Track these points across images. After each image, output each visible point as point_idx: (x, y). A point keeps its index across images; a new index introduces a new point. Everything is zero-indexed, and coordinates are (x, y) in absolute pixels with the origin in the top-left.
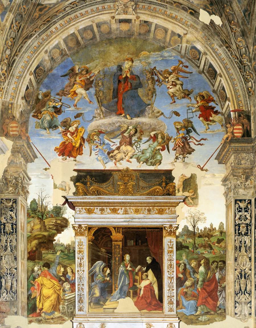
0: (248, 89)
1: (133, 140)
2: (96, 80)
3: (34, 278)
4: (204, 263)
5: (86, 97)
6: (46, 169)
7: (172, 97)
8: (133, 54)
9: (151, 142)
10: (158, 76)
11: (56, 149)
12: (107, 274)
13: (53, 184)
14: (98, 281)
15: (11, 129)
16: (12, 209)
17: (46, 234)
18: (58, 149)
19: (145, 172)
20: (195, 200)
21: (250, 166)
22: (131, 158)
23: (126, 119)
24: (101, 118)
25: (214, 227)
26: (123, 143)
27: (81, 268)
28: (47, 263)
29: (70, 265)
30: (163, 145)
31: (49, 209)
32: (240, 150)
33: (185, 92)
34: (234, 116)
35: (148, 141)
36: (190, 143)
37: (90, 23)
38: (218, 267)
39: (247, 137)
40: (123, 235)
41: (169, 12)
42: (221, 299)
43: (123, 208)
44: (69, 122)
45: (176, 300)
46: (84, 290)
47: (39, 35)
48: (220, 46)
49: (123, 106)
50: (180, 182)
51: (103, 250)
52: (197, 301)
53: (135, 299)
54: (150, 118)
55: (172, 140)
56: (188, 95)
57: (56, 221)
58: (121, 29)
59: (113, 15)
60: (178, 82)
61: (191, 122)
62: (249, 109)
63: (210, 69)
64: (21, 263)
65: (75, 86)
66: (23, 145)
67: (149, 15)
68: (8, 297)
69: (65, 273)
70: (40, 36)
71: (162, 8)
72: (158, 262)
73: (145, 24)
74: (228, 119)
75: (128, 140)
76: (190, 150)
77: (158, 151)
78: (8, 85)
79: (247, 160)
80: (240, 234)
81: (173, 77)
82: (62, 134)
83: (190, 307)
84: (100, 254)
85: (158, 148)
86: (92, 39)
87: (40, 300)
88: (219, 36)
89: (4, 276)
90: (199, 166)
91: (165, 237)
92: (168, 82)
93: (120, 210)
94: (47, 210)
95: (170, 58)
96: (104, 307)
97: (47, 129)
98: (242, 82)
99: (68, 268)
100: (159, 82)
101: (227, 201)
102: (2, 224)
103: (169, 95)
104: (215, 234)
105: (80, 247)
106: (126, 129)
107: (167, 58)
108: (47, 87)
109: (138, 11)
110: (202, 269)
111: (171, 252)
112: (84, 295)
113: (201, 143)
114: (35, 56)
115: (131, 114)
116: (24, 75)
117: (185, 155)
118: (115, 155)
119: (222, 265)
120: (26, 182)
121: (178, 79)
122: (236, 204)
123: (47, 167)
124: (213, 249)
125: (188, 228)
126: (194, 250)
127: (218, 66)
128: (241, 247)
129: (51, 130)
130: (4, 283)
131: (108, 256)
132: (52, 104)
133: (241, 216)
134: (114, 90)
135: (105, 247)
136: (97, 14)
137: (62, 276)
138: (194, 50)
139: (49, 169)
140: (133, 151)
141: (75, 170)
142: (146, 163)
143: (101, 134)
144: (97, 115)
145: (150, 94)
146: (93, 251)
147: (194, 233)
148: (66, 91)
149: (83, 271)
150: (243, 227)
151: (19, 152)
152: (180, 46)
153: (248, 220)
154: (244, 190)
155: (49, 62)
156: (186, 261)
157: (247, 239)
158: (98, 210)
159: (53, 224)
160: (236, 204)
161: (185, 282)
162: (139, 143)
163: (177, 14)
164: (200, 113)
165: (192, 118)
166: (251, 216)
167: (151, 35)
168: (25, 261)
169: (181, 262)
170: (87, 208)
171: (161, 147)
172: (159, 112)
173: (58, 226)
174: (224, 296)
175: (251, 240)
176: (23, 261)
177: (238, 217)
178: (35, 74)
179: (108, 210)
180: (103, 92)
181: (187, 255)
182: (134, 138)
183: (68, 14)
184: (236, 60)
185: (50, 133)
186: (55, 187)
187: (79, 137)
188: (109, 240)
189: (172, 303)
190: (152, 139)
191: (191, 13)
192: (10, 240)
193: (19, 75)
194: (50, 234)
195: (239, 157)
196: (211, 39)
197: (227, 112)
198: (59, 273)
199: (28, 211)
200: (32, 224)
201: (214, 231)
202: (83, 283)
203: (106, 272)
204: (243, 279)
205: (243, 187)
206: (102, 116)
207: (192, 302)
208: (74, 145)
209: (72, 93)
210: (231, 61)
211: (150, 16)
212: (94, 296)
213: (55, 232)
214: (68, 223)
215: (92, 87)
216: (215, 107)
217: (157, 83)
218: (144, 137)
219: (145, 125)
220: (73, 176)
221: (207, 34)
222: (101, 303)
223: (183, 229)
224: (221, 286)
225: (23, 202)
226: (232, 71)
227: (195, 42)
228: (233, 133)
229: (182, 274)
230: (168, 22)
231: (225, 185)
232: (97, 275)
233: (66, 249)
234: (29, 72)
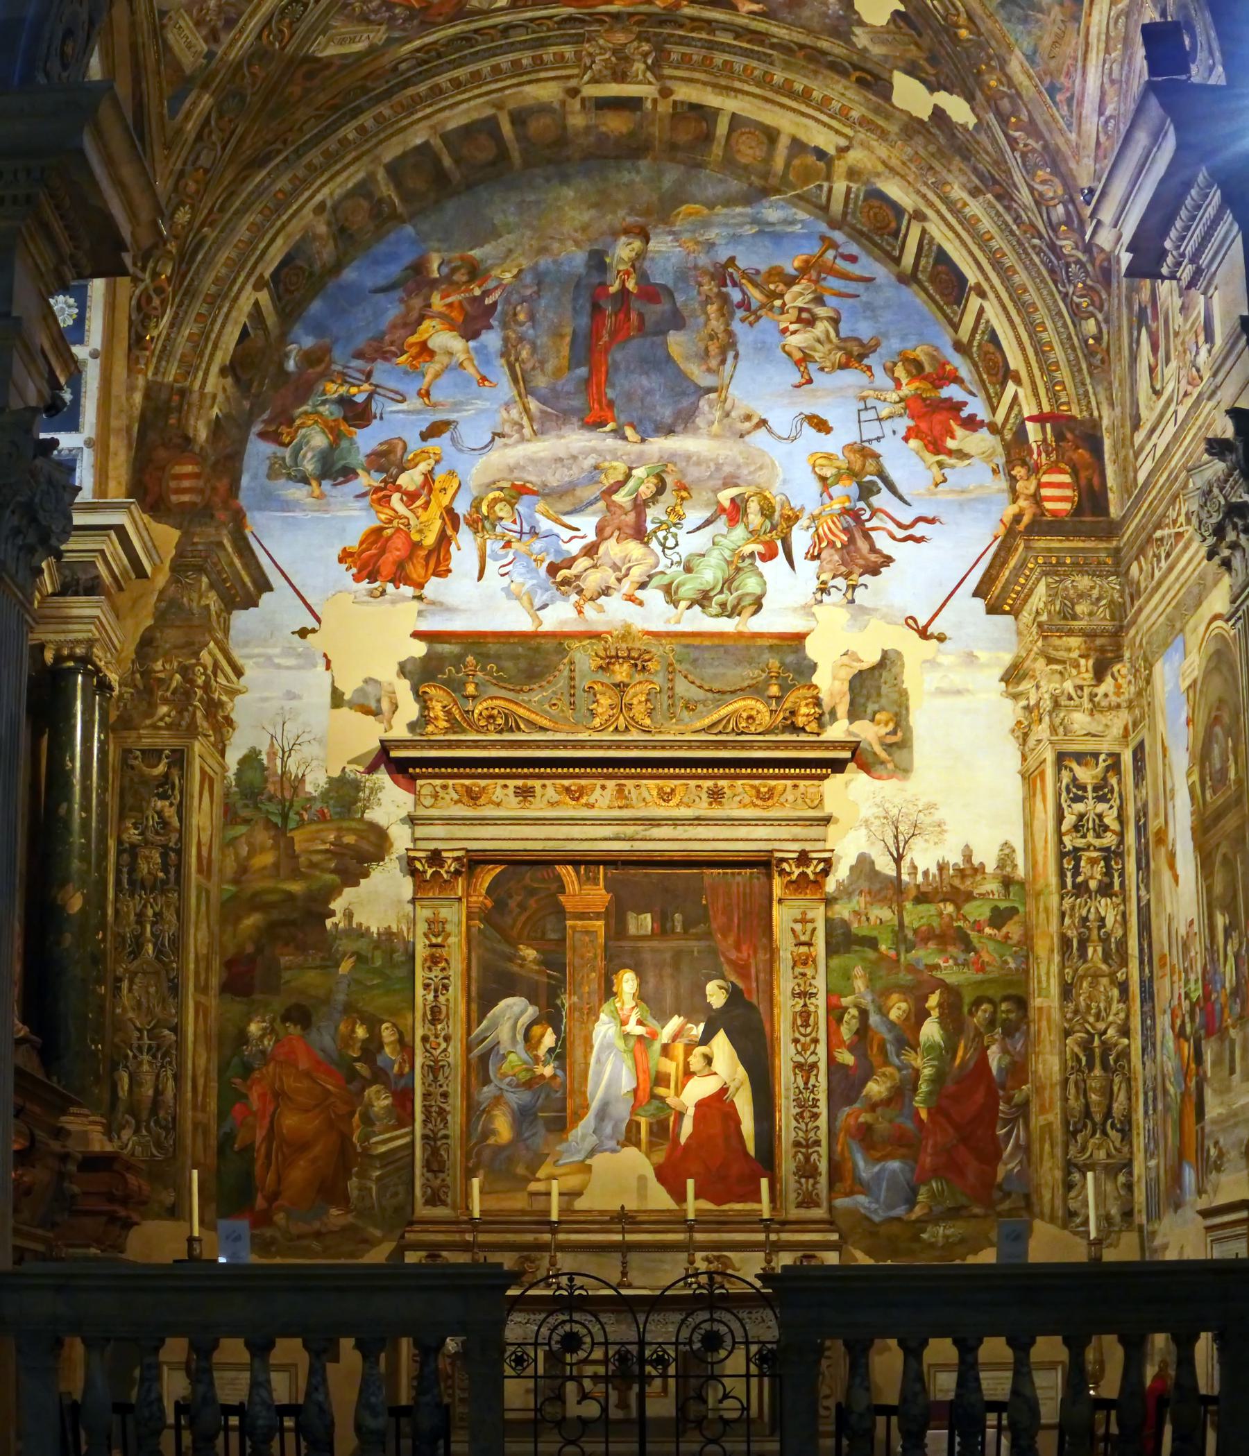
0: (1086, 341)
1: (649, 519)
2: (507, 301)
4: (940, 1005)
5: (466, 364)
6: (303, 633)
7: (797, 363)
8: (647, 212)
9: (721, 524)
10: (744, 293)
11: (345, 556)
12: (542, 1051)
13: (329, 690)
15: (173, 484)
16: (164, 787)
17: (296, 887)
18: (351, 555)
19: (697, 641)
20: (899, 755)
21: (1109, 625)
22: (643, 586)
23: (620, 442)
24: (523, 439)
25: (976, 861)
26: (608, 531)
30: (767, 538)
31: (309, 788)
32: (1068, 561)
33: (849, 345)
34: (1040, 437)
35: (708, 523)
36: (873, 534)
37: (489, 112)
38: (998, 1023)
39: (1093, 515)
41: (779, 77)
42: (1012, 1155)
43: (611, 784)
44: (399, 453)
45: (830, 1160)
46: (449, 1117)
47: (296, 151)
48: (975, 193)
49: (611, 394)
50: (837, 683)
51: (530, 954)
52: (916, 1161)
53: (660, 1157)
54: (716, 436)
55: (804, 521)
56: (861, 357)
57: (338, 838)
58: (604, 129)
59: (573, 83)
60: (820, 311)
61: (876, 456)
62: (1096, 414)
63: (940, 268)
64: (198, 1005)
65: (427, 324)
66: (221, 545)
67: (705, 83)
68: (139, 1143)
70: (299, 157)
71: (754, 64)
72: (755, 1001)
73: (692, 114)
74: (1016, 449)
75: (631, 518)
76: (873, 557)
77: (748, 561)
78: (172, 325)
79: (1098, 600)
80: (1081, 889)
81: (802, 294)
82: (368, 499)
83: (888, 1189)
85: (747, 549)
86: (493, 163)
87: (268, 1155)
88: (966, 158)
89: (127, 1056)
90: (910, 621)
91: (780, 901)
92: (783, 310)
93: (598, 790)
94: (302, 795)
95: (789, 229)
96: (534, 1186)
97: (314, 483)
98: (1062, 316)
100: (748, 309)
101: (1024, 758)
102: (125, 851)
103: (789, 354)
104: (982, 890)
105: (434, 940)
106: (621, 478)
107: (778, 228)
108: (318, 329)
109: (667, 71)
110: (931, 1031)
111: (806, 960)
112: (446, 1137)
113: (918, 535)
114: (279, 223)
115: (640, 421)
116: (236, 288)
117: (854, 577)
118: (577, 577)
119: (1012, 1016)
120: (224, 682)
121: (819, 300)
122: (1059, 771)
123: (310, 623)
124: (974, 949)
125: (873, 863)
126: (898, 954)
127: (970, 260)
128: (1088, 939)
129: (327, 484)
130: (126, 1087)
131: (549, 976)
132: (333, 390)
133: (1081, 816)
134: (574, 333)
135: (535, 939)
136: (515, 81)
137: (357, 1060)
138: (876, 203)
139: (314, 631)
140: (651, 560)
141: (417, 635)
142: (703, 606)
143: (526, 498)
144: (507, 429)
145: (714, 349)
147: (897, 886)
148: (392, 343)
149: (447, 1039)
150: (1093, 862)
151: (200, 570)
152: (825, 189)
153: (1109, 834)
154: (1092, 714)
155: (331, 243)
156: (869, 998)
157: (1110, 907)
158: (511, 791)
159: (327, 846)
160: (1059, 771)
161: (863, 1084)
162: (673, 530)
163: (806, 82)
164: (907, 422)
165: (878, 439)
166: (1121, 819)
167: (717, 150)
168: (213, 1001)
169: (845, 1001)
171: (759, 548)
172: (748, 418)
173: (343, 855)
174: (1022, 1142)
175: (1124, 914)
176: (203, 999)
177: (1070, 820)
178: (276, 286)
180: (534, 349)
182: (653, 514)
183: (407, 83)
184: (1036, 241)
185: (322, 496)
186: (337, 699)
187: (435, 511)
189: (813, 1173)
190: (724, 517)
191: (861, 82)
192: (155, 915)
193: (213, 289)
194: (314, 887)
195: (1066, 589)
196: (937, 166)
197: (1011, 420)
199: (227, 795)
200: (244, 850)
201: (979, 878)
203: (539, 1042)
204: (1098, 1072)
205: (1087, 705)
206: (527, 431)
207: (895, 1165)
208: (415, 537)
209: (414, 351)
210: (1019, 241)
211: (709, 89)
212: (491, 1141)
215: (490, 327)
216: (965, 404)
217: (740, 313)
218: (693, 507)
219: (698, 464)
220: (412, 659)
221: (922, 152)
222: (521, 1170)
223: (852, 868)
224: (1009, 1100)
225: (210, 761)
226: (1022, 277)
227: (878, 175)
228: (1037, 499)
229: (851, 1049)
230: (777, 109)
231: (1015, 697)
232: (504, 1057)
233: (376, 947)
234: (253, 280)
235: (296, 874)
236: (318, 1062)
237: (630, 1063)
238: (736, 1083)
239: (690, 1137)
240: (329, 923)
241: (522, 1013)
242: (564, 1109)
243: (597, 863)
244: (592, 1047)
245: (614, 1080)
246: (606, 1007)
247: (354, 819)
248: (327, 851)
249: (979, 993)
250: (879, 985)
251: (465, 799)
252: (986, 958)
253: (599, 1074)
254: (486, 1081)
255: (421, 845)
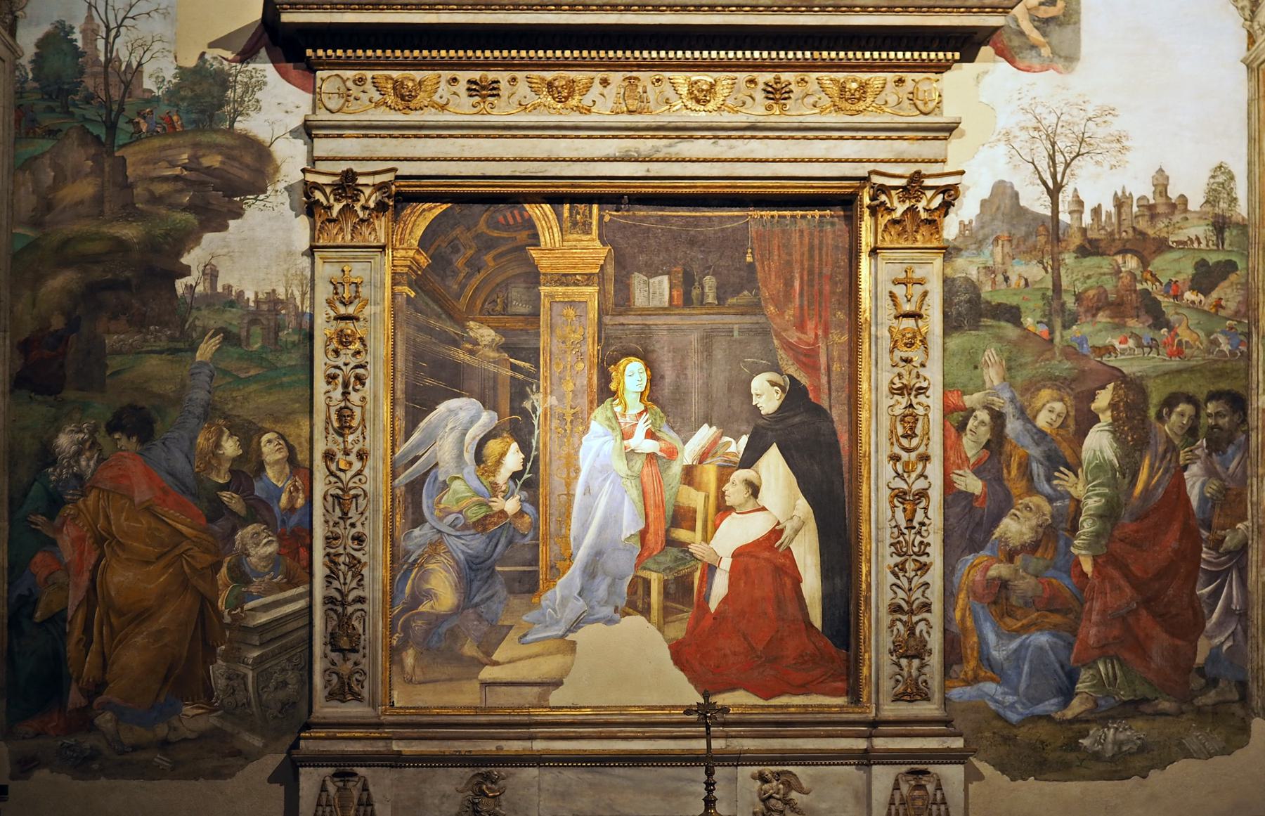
3: (54, 503)
12: (503, 476)
14: (451, 518)
27: (350, 438)
28: (134, 409)
29: (277, 420)
40: (604, 244)
69: (245, 469)
84: (462, 356)
99: (265, 438)
105: (342, 310)
137: (225, 487)
146: (422, 338)
149: (362, 456)
156: (1007, 395)
158: (462, 87)
169: (969, 400)
170: (388, 78)
173: (203, 183)
179: (523, 89)
181: (1009, 360)
188: (519, 275)
198: (209, 467)
202: (359, 529)
203: (499, 462)
213: (191, 218)
214: (270, 170)
232: (445, 486)
233: (254, 322)
235: (129, 213)
236: (165, 492)
237: (634, 493)
238: (795, 523)
239: (725, 601)
240: (180, 285)
241: (472, 422)
242: (535, 561)
243: (589, 199)
244: (578, 471)
245: (611, 519)
246: (600, 413)
247: (217, 131)
248: (177, 178)
249: (1173, 388)
250: (1021, 377)
251: (390, 99)
252: (1184, 335)
253: (588, 511)
254: (418, 520)
255: (321, 166)
